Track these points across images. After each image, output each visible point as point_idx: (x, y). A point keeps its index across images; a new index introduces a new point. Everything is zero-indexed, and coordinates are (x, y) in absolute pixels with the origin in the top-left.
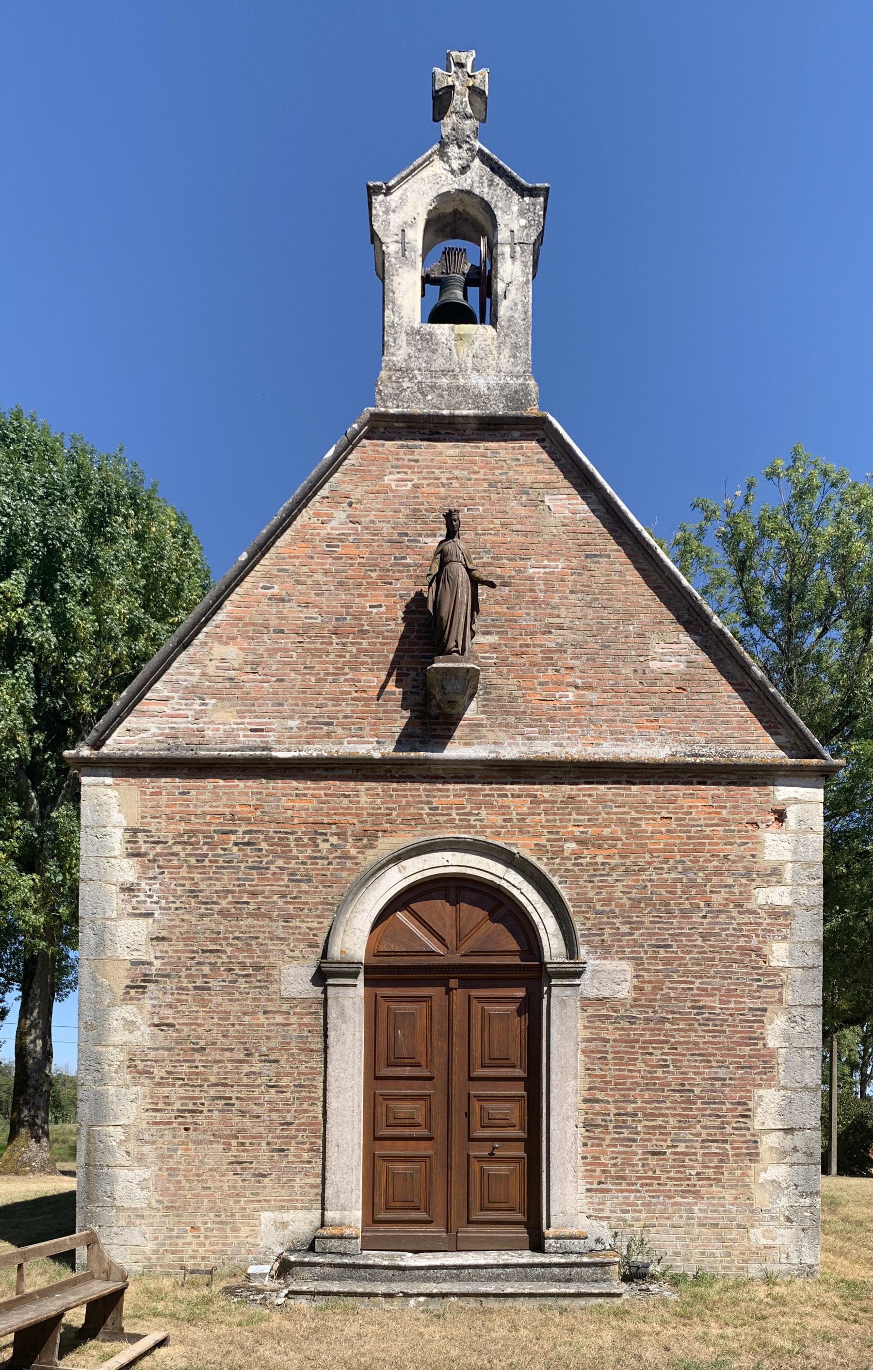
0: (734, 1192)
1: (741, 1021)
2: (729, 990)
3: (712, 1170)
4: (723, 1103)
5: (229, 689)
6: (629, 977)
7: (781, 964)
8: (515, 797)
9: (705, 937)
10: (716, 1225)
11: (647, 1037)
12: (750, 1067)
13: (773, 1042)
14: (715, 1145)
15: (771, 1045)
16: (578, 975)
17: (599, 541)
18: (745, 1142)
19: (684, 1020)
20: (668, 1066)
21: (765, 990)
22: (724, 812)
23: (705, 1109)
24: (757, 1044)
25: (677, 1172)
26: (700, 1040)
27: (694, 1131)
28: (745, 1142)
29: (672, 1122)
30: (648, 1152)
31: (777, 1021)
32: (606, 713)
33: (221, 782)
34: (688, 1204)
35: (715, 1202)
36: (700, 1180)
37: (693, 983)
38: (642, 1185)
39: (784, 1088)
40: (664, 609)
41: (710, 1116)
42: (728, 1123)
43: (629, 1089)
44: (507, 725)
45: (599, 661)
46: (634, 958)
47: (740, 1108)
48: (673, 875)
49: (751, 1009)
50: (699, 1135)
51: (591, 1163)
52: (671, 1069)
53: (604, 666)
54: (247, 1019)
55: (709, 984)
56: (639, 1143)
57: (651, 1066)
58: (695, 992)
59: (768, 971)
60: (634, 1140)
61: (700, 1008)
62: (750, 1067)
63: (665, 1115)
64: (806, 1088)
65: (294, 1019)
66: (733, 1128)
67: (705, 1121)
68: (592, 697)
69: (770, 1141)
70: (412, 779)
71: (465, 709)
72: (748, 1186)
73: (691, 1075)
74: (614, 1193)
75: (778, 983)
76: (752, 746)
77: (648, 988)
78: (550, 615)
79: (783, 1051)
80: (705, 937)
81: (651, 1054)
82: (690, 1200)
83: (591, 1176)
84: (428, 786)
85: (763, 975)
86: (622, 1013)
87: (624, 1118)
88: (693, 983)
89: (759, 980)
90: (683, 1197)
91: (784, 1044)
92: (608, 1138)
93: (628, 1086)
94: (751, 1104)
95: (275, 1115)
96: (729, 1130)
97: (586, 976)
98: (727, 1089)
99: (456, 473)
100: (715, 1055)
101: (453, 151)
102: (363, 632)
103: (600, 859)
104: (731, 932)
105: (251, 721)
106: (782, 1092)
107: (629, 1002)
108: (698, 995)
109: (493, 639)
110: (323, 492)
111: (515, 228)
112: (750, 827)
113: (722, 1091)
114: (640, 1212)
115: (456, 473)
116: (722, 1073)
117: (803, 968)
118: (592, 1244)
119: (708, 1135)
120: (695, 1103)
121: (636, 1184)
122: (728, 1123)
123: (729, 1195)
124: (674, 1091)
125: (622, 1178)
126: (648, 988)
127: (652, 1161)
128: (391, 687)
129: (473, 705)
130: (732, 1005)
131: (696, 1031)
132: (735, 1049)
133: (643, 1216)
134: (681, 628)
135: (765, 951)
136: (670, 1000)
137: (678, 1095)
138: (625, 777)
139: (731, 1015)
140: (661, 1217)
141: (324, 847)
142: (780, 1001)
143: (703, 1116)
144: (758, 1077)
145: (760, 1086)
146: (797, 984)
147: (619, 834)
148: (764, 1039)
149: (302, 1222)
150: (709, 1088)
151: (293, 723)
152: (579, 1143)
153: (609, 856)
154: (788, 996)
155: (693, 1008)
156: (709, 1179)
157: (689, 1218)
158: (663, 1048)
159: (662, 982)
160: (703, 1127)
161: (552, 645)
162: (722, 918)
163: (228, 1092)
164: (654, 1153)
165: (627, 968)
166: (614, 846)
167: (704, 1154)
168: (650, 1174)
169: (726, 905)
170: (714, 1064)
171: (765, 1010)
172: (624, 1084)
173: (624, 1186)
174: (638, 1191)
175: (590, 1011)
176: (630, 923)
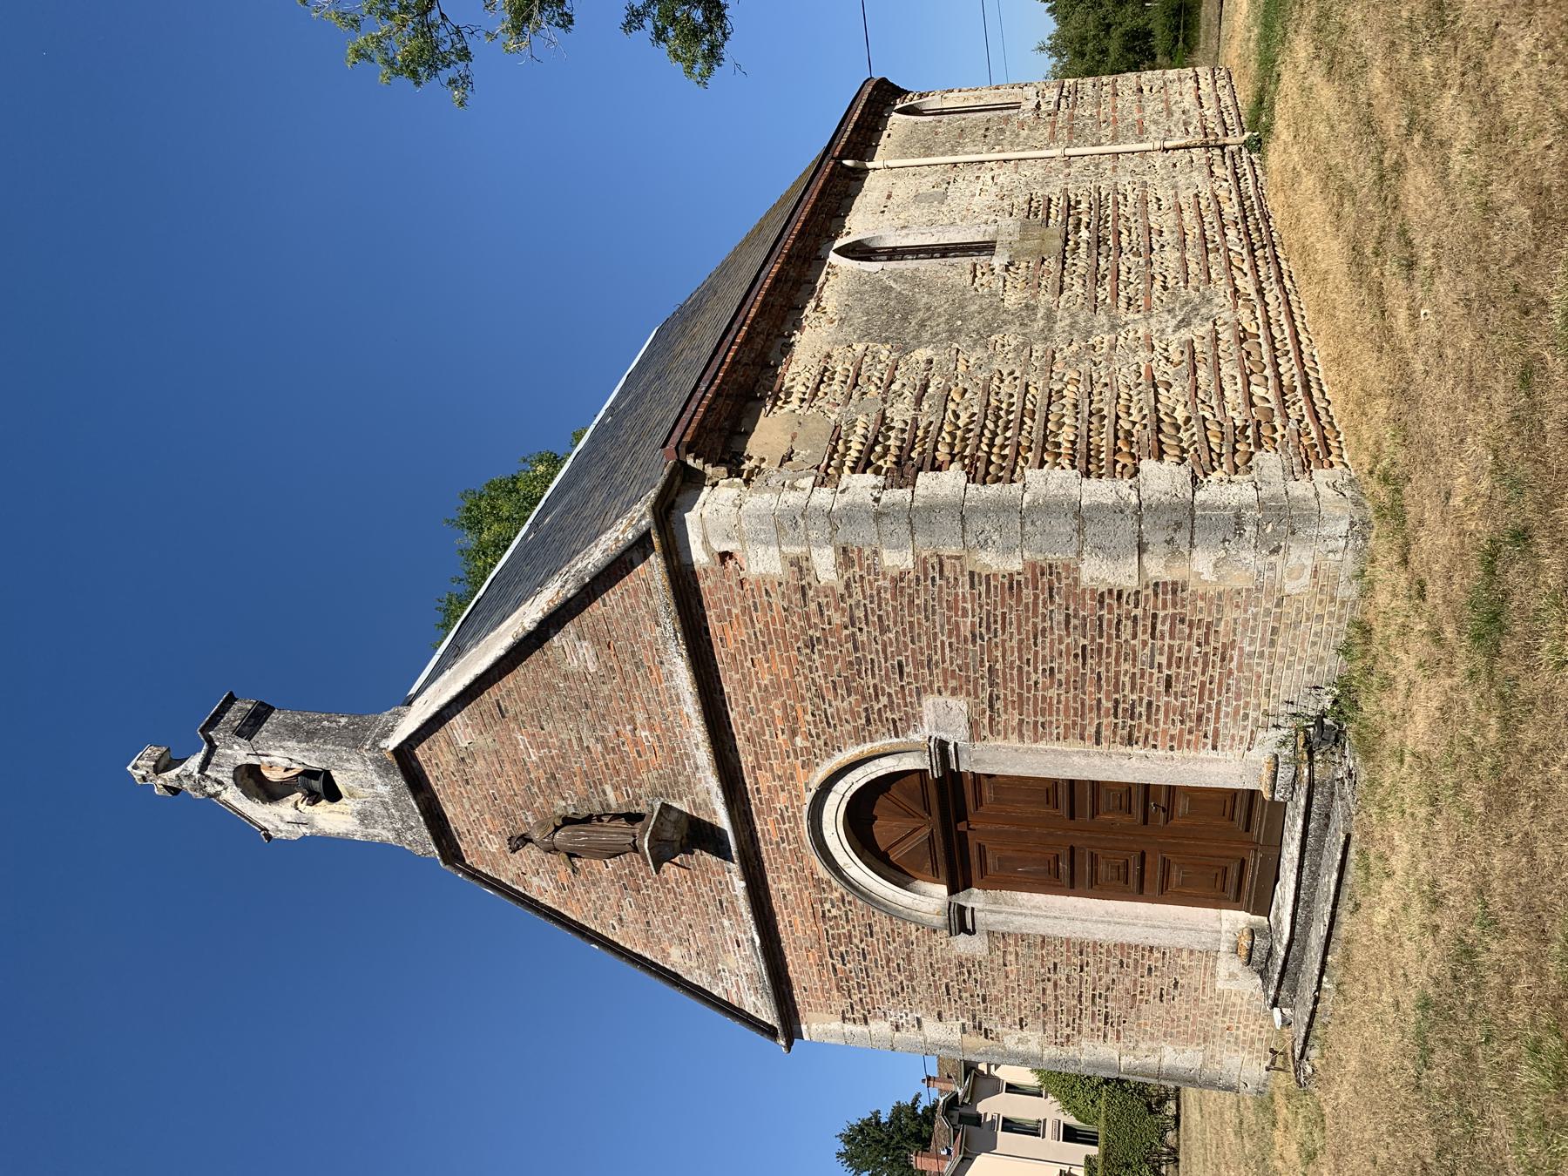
0: (1226, 610)
1: (988, 595)
2: (949, 609)
3: (1195, 631)
4: (1100, 618)
5: (709, 955)
6: (941, 700)
7: (910, 558)
8: (758, 782)
9: (884, 630)
10: (1274, 631)
11: (1015, 686)
12: (1051, 589)
13: (1015, 565)
14: (1159, 627)
15: (1019, 567)
16: (942, 745)
17: (484, 707)
18: (1156, 595)
19: (990, 651)
20: (1052, 669)
21: (946, 573)
22: (735, 611)
23: (1109, 636)
24: (1019, 583)
25: (1195, 664)
26: (1016, 637)
27: (1139, 647)
28: (1156, 595)
29: (1125, 666)
30: (1167, 691)
31: (987, 561)
32: (653, 707)
33: (790, 968)
34: (1241, 656)
35: (1240, 629)
36: (1207, 642)
37: (943, 643)
38: (1211, 698)
39: (1079, 553)
40: (533, 657)
41: (1118, 630)
42: (1128, 612)
43: (1083, 704)
44: (689, 783)
45: (602, 711)
46: (919, 694)
47: (1107, 601)
48: (816, 657)
49: (972, 586)
50: (1145, 643)
51: (1175, 743)
52: (1055, 665)
53: (607, 707)
54: (1012, 977)
55: (942, 627)
56: (1153, 698)
57: (1052, 684)
58: (954, 640)
59: (921, 569)
60: (1150, 704)
61: (974, 636)
62: (1051, 589)
63: (1117, 674)
64: (1080, 531)
65: (1011, 949)
66: (1136, 606)
67: (1126, 634)
68: (640, 718)
69: (1155, 567)
70: (758, 853)
71: (681, 812)
72: (1220, 596)
73: (1063, 647)
74: (1221, 725)
75: (935, 559)
76: (652, 584)
77: (953, 683)
78: (571, 746)
79: (1027, 554)
80: (884, 630)
81: (1036, 683)
82: (1236, 653)
83: (1196, 744)
84: (762, 844)
85: (926, 575)
86: (986, 706)
87: (1120, 711)
88: (943, 643)
89: (933, 579)
90: (1232, 659)
91: (1018, 552)
92: (1146, 726)
93: (1079, 705)
94: (1103, 588)
95: (1111, 970)
96: (1139, 612)
97: (944, 737)
98: (1082, 613)
99: (467, 806)
100: (1035, 625)
101: (210, 790)
102: (631, 874)
103: (809, 718)
104: (875, 606)
105: (731, 946)
106: (1085, 556)
107: (971, 699)
108: (958, 636)
109: (608, 788)
110: (521, 889)
111: (244, 753)
112: (747, 586)
113: (1084, 618)
114: (1247, 703)
115: (467, 806)
116: (1059, 617)
117: (913, 534)
118: (1287, 751)
119: (1144, 632)
120: (1101, 645)
121: (1209, 706)
122: (1128, 612)
123: (1230, 614)
124: (1084, 664)
125: (1199, 718)
126: (953, 683)
127: (1177, 687)
128: (677, 860)
129: (675, 805)
130: (969, 606)
131: (1004, 641)
132: (1027, 605)
133: (1253, 701)
134: (546, 645)
135: (896, 573)
136: (967, 664)
137: (1089, 661)
138: (717, 696)
139: (981, 607)
140: (1257, 684)
141: (834, 912)
142: (958, 558)
143: (1118, 637)
144: (1064, 582)
145: (1076, 580)
146: (934, 540)
147: (779, 702)
148: (1011, 575)
149: (1229, 965)
150: (1080, 630)
151: (726, 923)
152: (1151, 752)
153: (805, 712)
154: (953, 550)
155: (974, 641)
156: (1207, 634)
157: (1262, 655)
158: (1028, 673)
159: (945, 671)
160: (1134, 636)
161: (599, 747)
162: (860, 613)
163: (1087, 994)
164: (1168, 686)
165: (931, 701)
166: (793, 708)
167: (1172, 637)
168: (1196, 691)
169: (844, 610)
170: (1048, 624)
171: (972, 574)
172: (1076, 709)
173: (1212, 716)
174: (1219, 703)
175: (986, 732)
176: (877, 695)
